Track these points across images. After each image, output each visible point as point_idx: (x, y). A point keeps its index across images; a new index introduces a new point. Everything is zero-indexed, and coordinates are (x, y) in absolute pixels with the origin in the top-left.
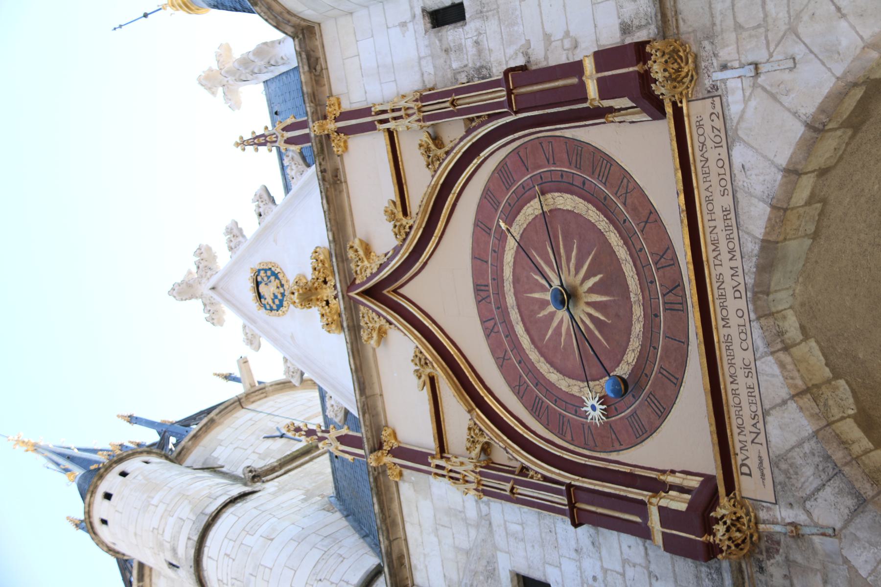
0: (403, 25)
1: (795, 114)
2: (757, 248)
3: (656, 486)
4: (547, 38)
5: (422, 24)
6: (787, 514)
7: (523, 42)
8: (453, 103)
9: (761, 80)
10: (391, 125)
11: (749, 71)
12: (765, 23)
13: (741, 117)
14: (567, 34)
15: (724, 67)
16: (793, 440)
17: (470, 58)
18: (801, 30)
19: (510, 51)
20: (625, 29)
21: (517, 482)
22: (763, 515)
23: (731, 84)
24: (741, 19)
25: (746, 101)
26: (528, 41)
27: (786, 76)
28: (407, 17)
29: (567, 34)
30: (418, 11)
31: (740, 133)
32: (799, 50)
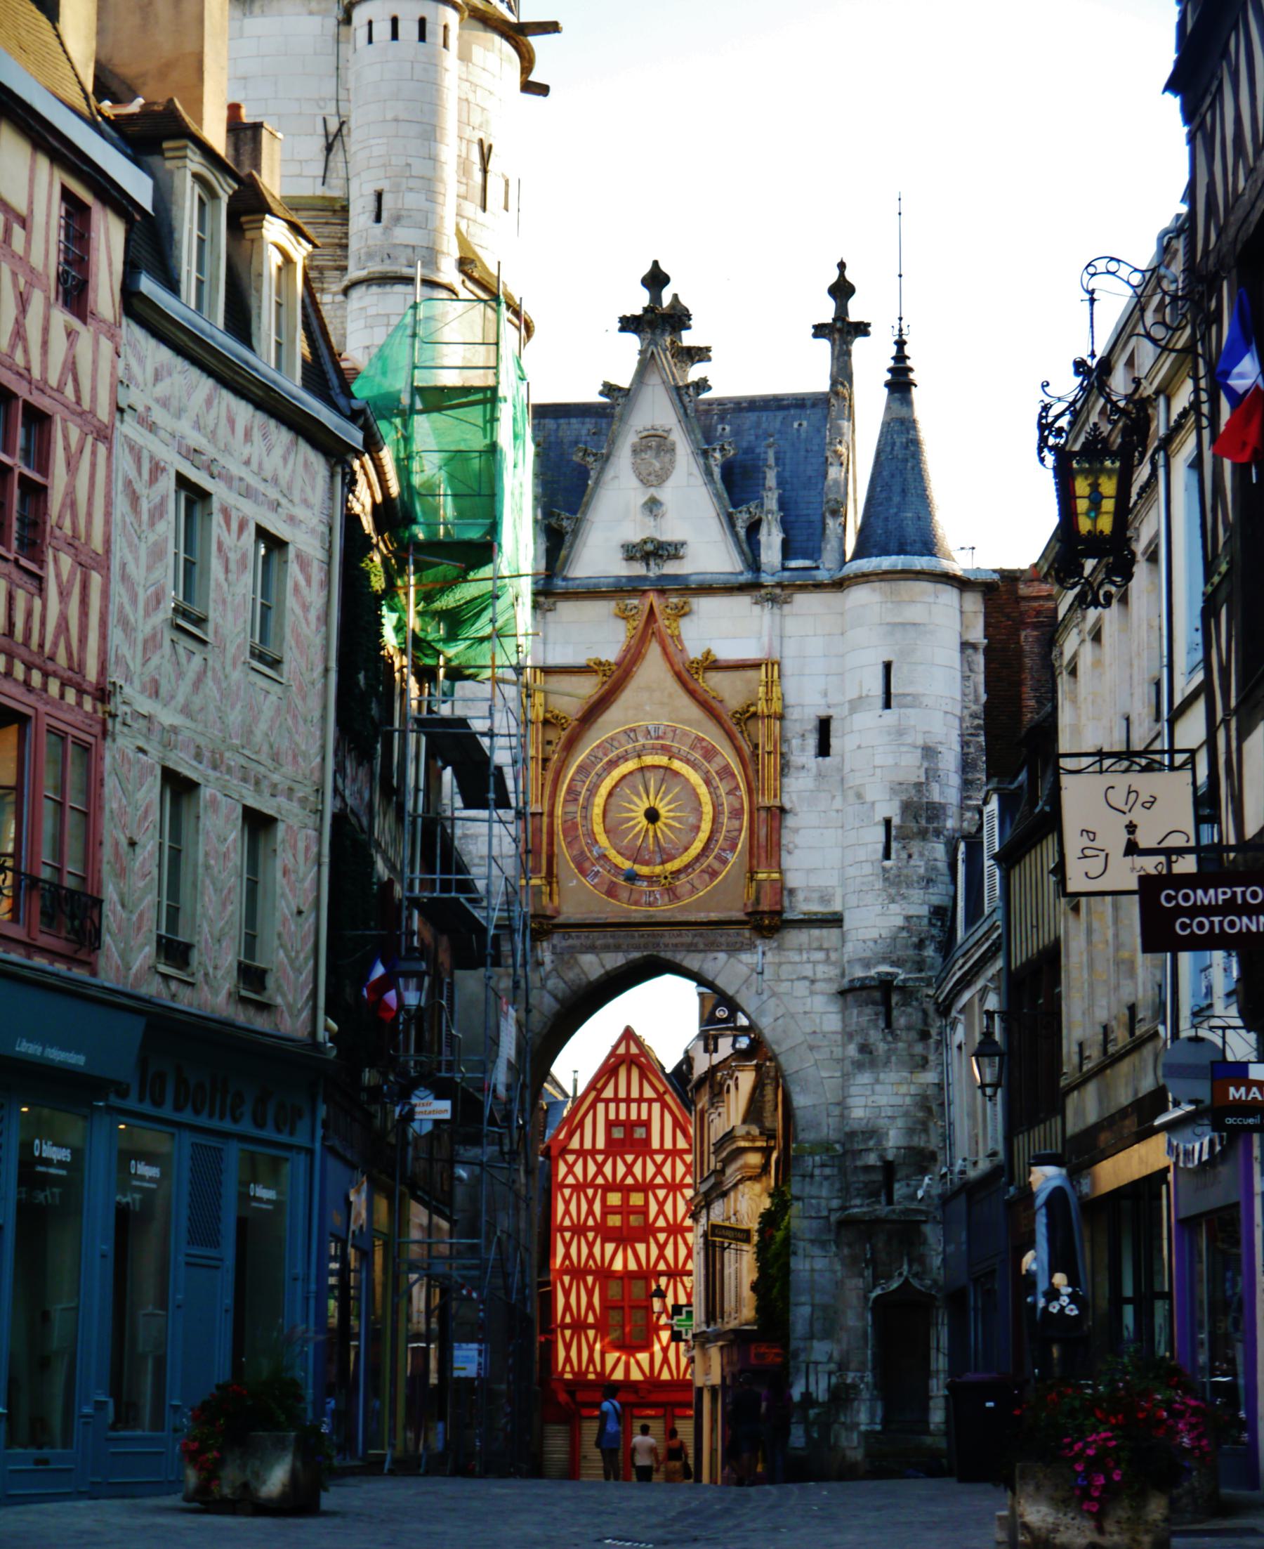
0: (825, 695)
1: (737, 992)
2: (677, 961)
3: (550, 874)
4: (796, 831)
5: (823, 713)
6: (548, 958)
7: (798, 809)
8: (769, 753)
9: (755, 975)
10: (763, 667)
11: (759, 969)
12: (779, 980)
13: (740, 961)
14: (796, 847)
15: (764, 953)
16: (586, 968)
17: (797, 759)
18: (773, 999)
19: (794, 798)
20: (792, 892)
21: (537, 759)
22: (545, 944)
23: (755, 957)
24: (784, 967)
25: (747, 964)
26: (796, 815)
27: (754, 989)
28: (833, 699)
29: (796, 847)
30: (831, 712)
31: (732, 960)
32: (765, 997)
